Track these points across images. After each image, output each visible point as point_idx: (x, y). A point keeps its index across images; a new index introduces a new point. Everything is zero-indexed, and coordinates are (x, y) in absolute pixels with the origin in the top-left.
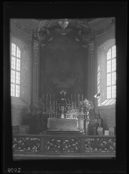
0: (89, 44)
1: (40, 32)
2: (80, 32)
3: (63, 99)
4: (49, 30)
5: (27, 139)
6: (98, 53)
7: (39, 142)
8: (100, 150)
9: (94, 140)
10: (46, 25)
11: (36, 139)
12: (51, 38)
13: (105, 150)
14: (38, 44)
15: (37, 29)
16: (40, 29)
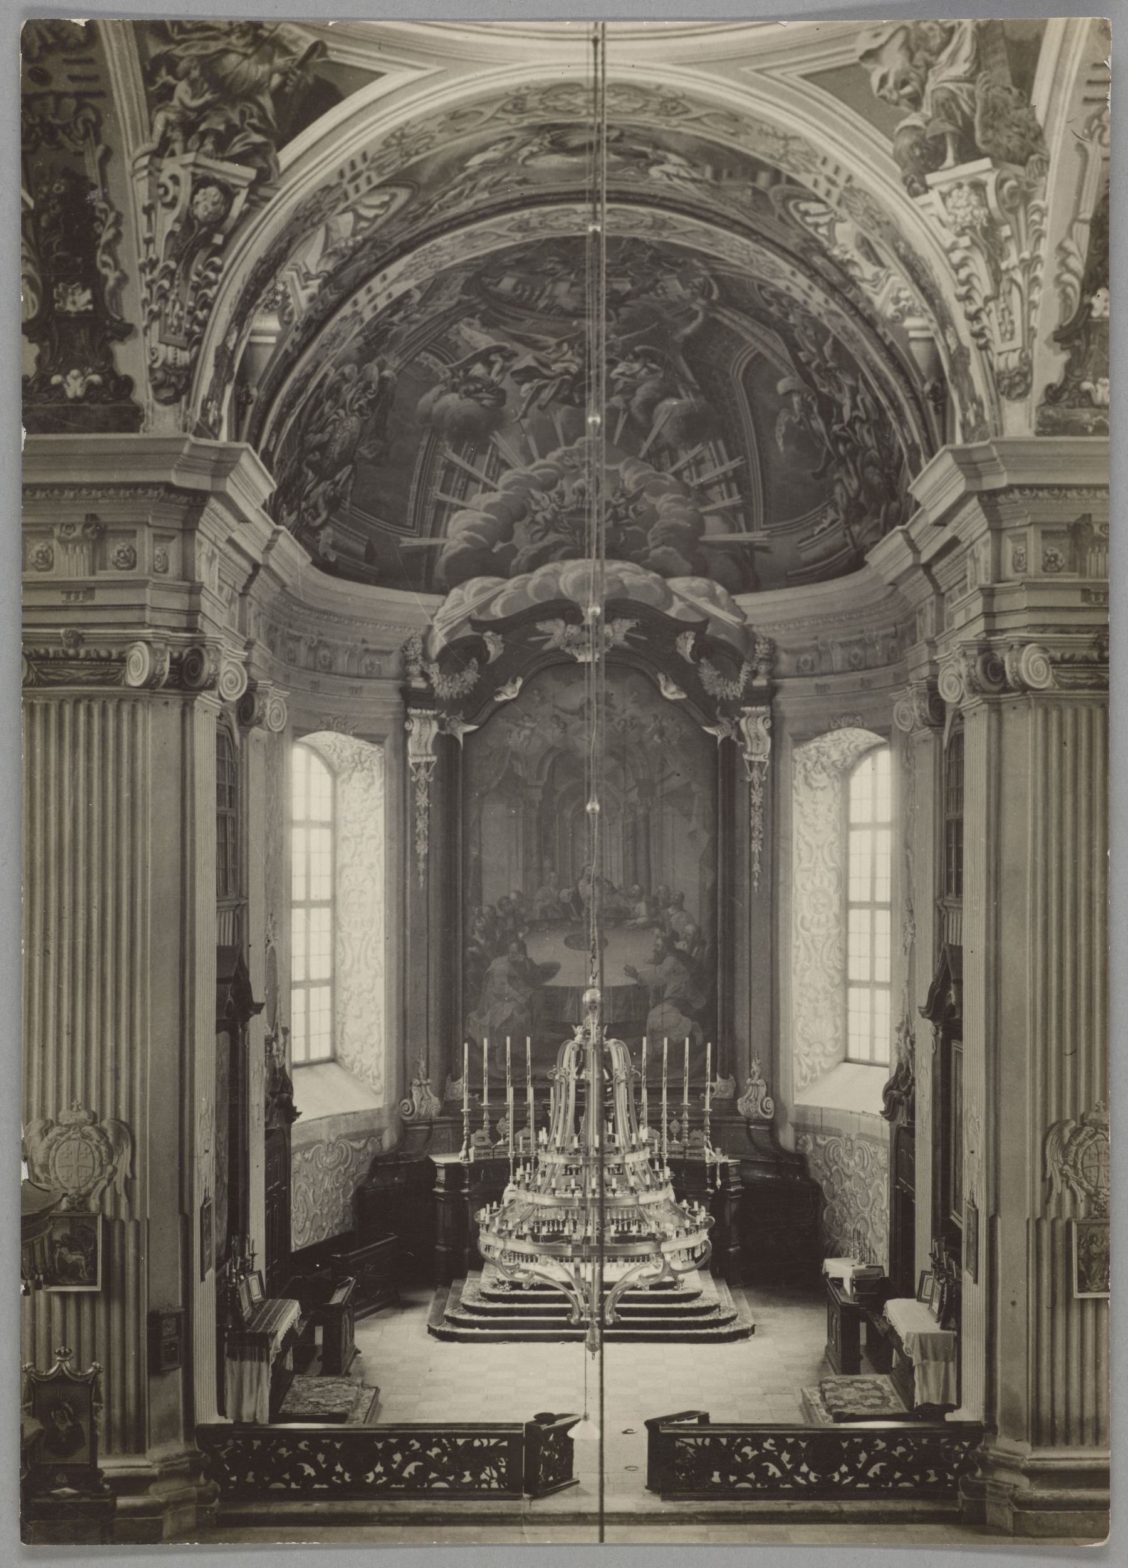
1: (444, 651)
2: (686, 645)
4: (497, 631)
5: (460, 1442)
6: (799, 781)
7: (502, 1451)
8: (732, 1478)
9: (707, 1441)
10: (484, 607)
11: (493, 1441)
12: (514, 682)
13: (749, 1480)
14: (435, 728)
15: (426, 639)
16: (447, 634)
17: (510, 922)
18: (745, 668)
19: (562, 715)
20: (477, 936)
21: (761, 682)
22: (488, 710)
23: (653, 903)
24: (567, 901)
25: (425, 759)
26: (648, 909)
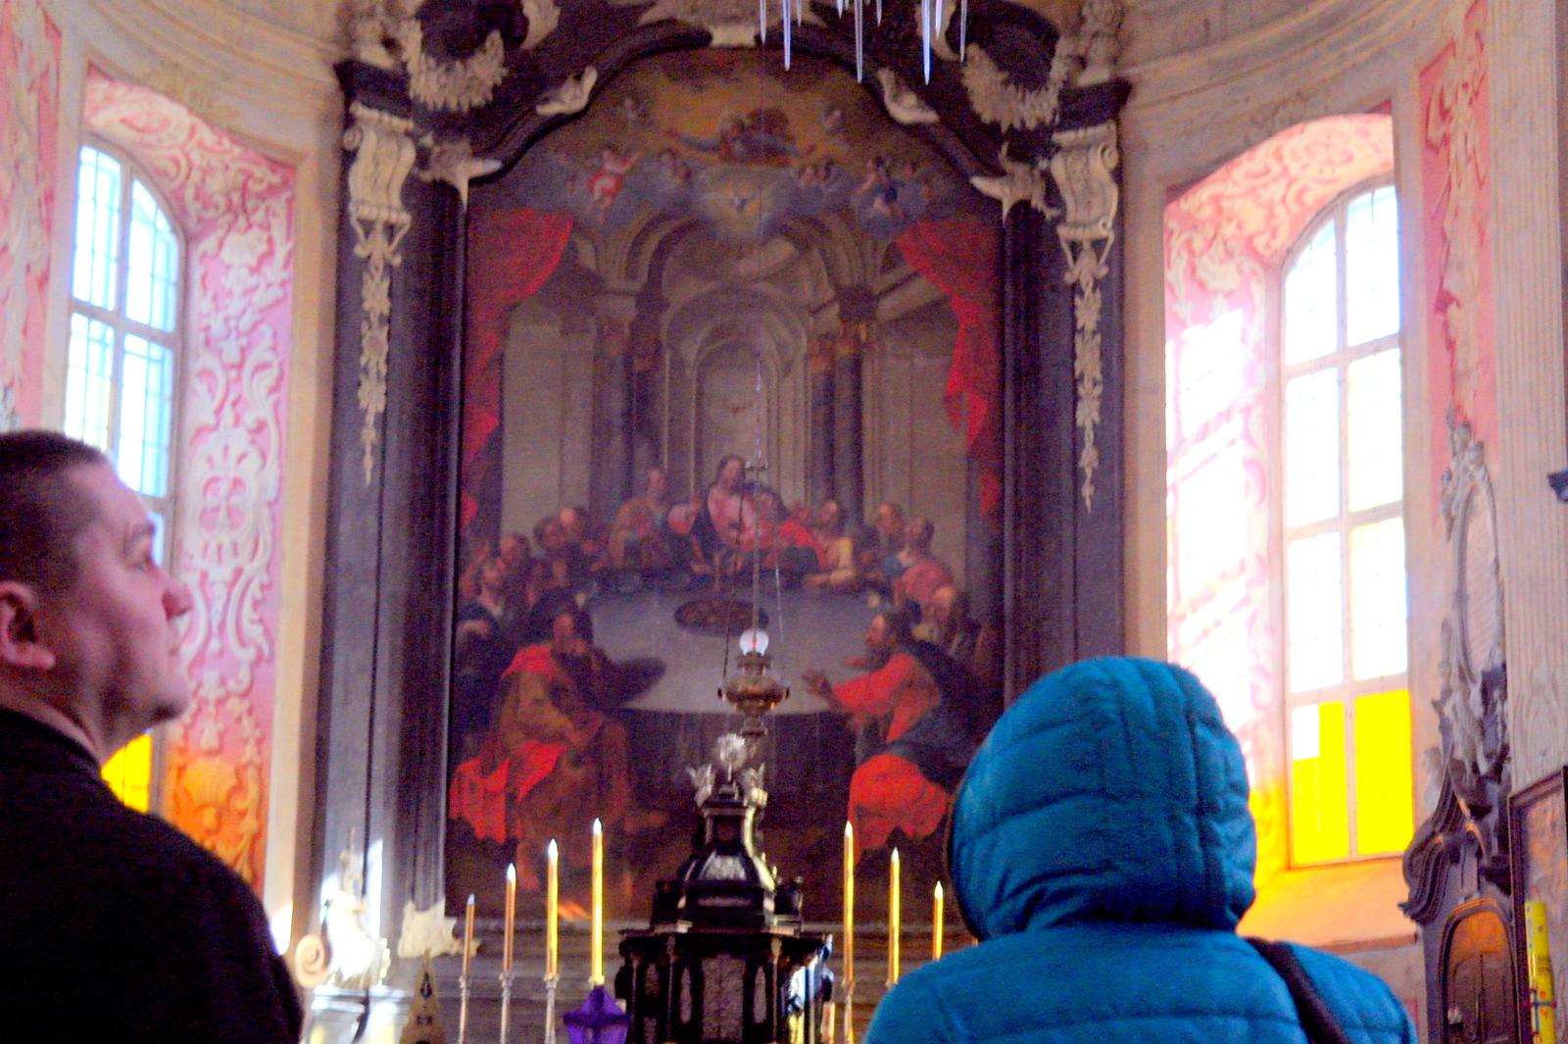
0: (1058, 167)
3: (721, 867)
6: (1175, 273)
12: (579, 78)
14: (409, 154)
17: (559, 570)
18: (1063, 47)
19: (681, 148)
20: (486, 600)
21: (1096, 75)
22: (522, 133)
23: (866, 540)
24: (683, 531)
25: (384, 215)
26: (856, 554)
